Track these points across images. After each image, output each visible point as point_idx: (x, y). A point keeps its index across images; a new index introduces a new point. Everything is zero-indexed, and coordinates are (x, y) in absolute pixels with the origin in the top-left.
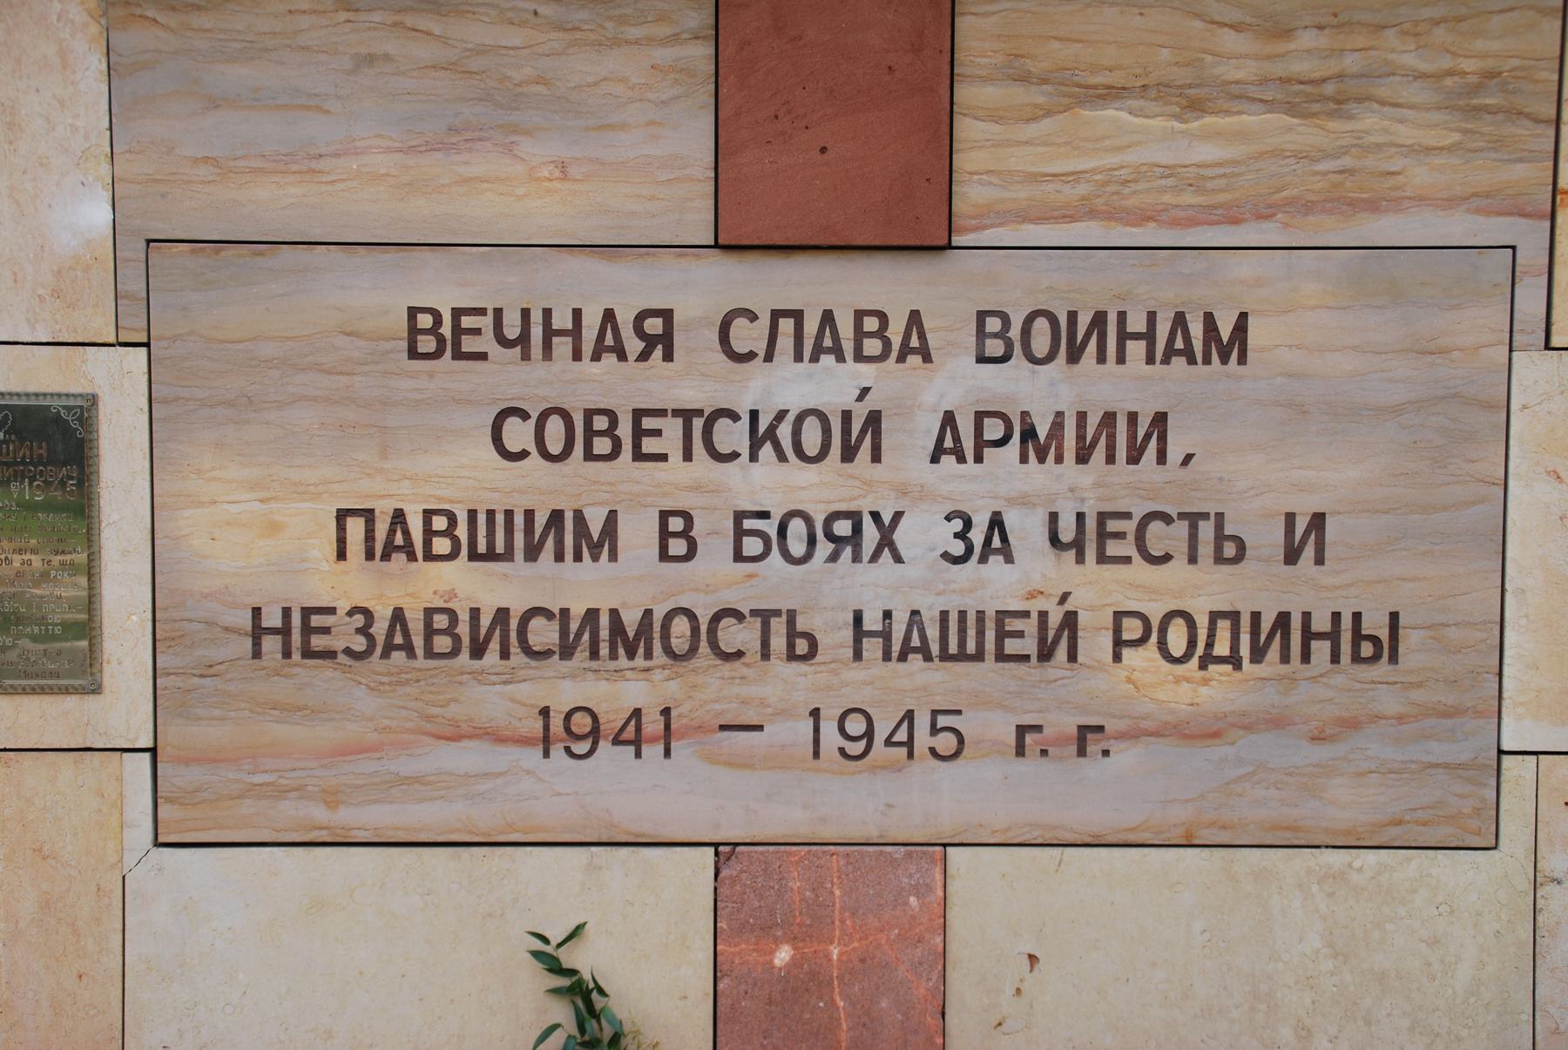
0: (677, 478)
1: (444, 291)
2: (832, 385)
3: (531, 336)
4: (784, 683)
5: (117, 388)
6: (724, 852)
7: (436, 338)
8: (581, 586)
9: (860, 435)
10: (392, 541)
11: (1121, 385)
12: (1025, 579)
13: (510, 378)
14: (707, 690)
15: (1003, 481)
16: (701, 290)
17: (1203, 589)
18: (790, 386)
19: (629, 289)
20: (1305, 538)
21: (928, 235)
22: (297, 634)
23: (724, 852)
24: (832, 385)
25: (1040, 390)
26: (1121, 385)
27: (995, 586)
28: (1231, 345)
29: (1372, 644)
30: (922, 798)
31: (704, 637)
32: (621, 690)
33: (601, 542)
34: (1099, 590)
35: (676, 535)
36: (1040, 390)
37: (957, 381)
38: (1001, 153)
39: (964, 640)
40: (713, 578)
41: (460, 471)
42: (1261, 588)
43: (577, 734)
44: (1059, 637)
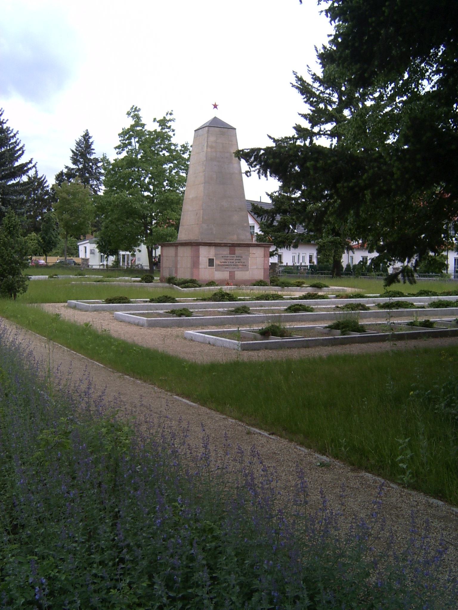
5: (215, 258)
8: (227, 264)
12: (237, 264)
15: (237, 261)
16: (229, 256)
19: (227, 256)
22: (219, 265)
25: (237, 258)
30: (235, 270)
31: (229, 265)
34: (239, 264)
36: (237, 258)
37: (235, 258)
39: (236, 265)
41: (223, 261)
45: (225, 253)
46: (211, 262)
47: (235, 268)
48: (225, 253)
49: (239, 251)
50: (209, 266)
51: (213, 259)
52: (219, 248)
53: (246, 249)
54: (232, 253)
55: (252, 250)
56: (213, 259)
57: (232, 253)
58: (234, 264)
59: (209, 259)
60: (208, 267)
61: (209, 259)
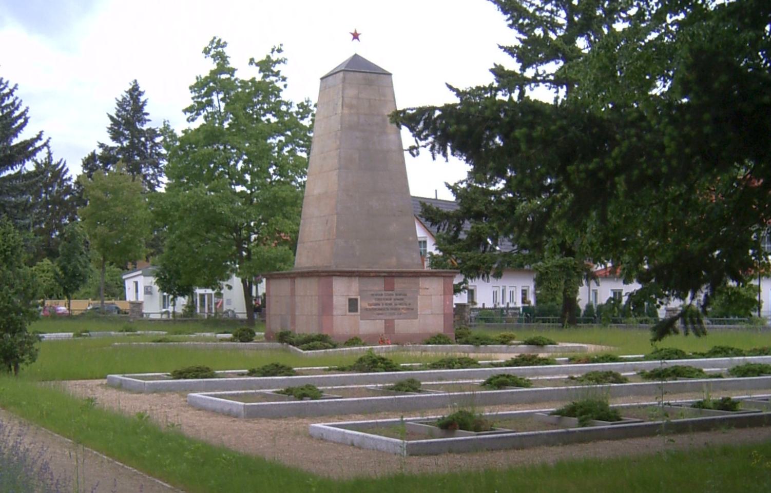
0: (383, 302)
1: (373, 293)
2: (389, 297)
3: (376, 295)
4: (387, 311)
5: (359, 297)
6: (385, 320)
7: (372, 295)
8: (381, 307)
9: (391, 299)
10: (370, 305)
11: (401, 297)
13: (376, 297)
14: (384, 312)
15: (398, 302)
16: (383, 293)
17: (405, 307)
18: (387, 297)
19: (380, 293)
20: (410, 304)
21: (393, 290)
22: (366, 309)
23: (385, 320)
24: (389, 297)
25: (399, 297)
26: (401, 297)
27: (396, 307)
28: (406, 295)
29: (413, 309)
30: (394, 317)
32: (381, 312)
33: (379, 305)
34: (401, 307)
35: (383, 305)
36: (399, 297)
37: (394, 297)
38: (396, 286)
39: (396, 309)
40: (384, 306)
41: (374, 301)
42: (408, 307)
43: (379, 314)
44: (399, 309)
45: (376, 288)
46: (353, 305)
47: (394, 314)
48: (376, 288)
49: (399, 284)
50: (350, 311)
51: (356, 300)
52: (366, 279)
53: (412, 280)
54: (389, 287)
55: (424, 283)
56: (356, 300)
57: (389, 287)
58: (393, 306)
59: (350, 300)
60: (348, 313)
61: (350, 300)
